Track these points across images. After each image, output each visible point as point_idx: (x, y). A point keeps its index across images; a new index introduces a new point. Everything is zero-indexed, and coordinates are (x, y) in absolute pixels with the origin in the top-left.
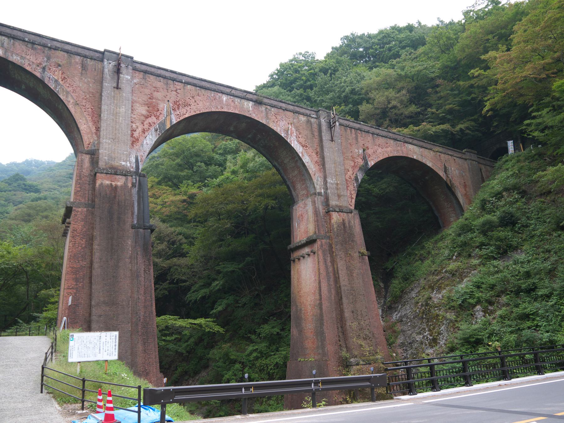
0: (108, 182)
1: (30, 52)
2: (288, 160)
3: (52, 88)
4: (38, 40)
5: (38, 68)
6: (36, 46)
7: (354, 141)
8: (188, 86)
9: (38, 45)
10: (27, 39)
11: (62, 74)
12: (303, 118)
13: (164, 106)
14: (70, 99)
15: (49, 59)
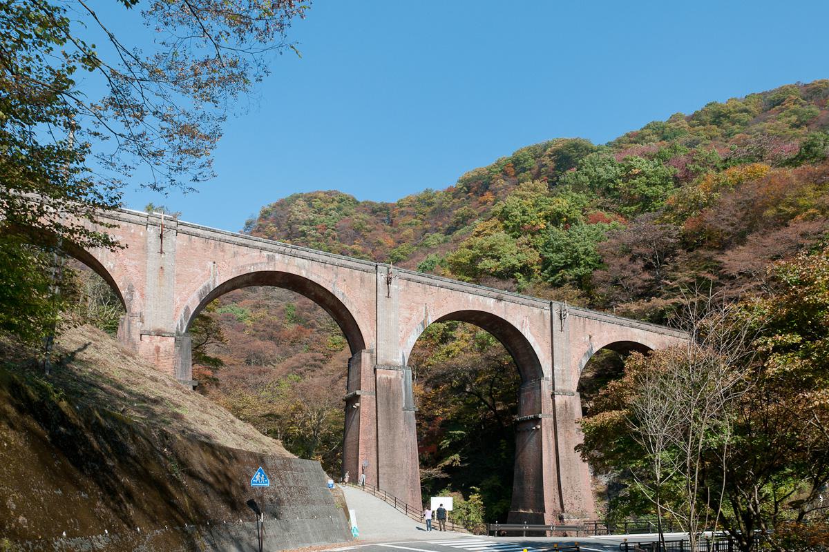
0: (384, 376)
1: (324, 270)
2: (521, 346)
6: (327, 265)
7: (582, 329)
8: (442, 289)
10: (321, 261)
12: (537, 311)
13: (422, 311)
14: (353, 308)
15: (337, 276)
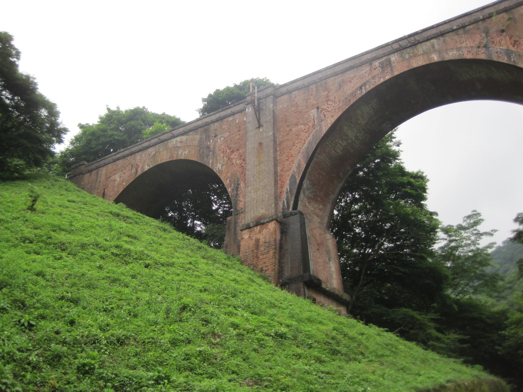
3: (505, 62)
4: (467, 20)
5: (480, 49)
6: (467, 28)
9: (469, 25)
11: (510, 38)
15: (487, 32)
